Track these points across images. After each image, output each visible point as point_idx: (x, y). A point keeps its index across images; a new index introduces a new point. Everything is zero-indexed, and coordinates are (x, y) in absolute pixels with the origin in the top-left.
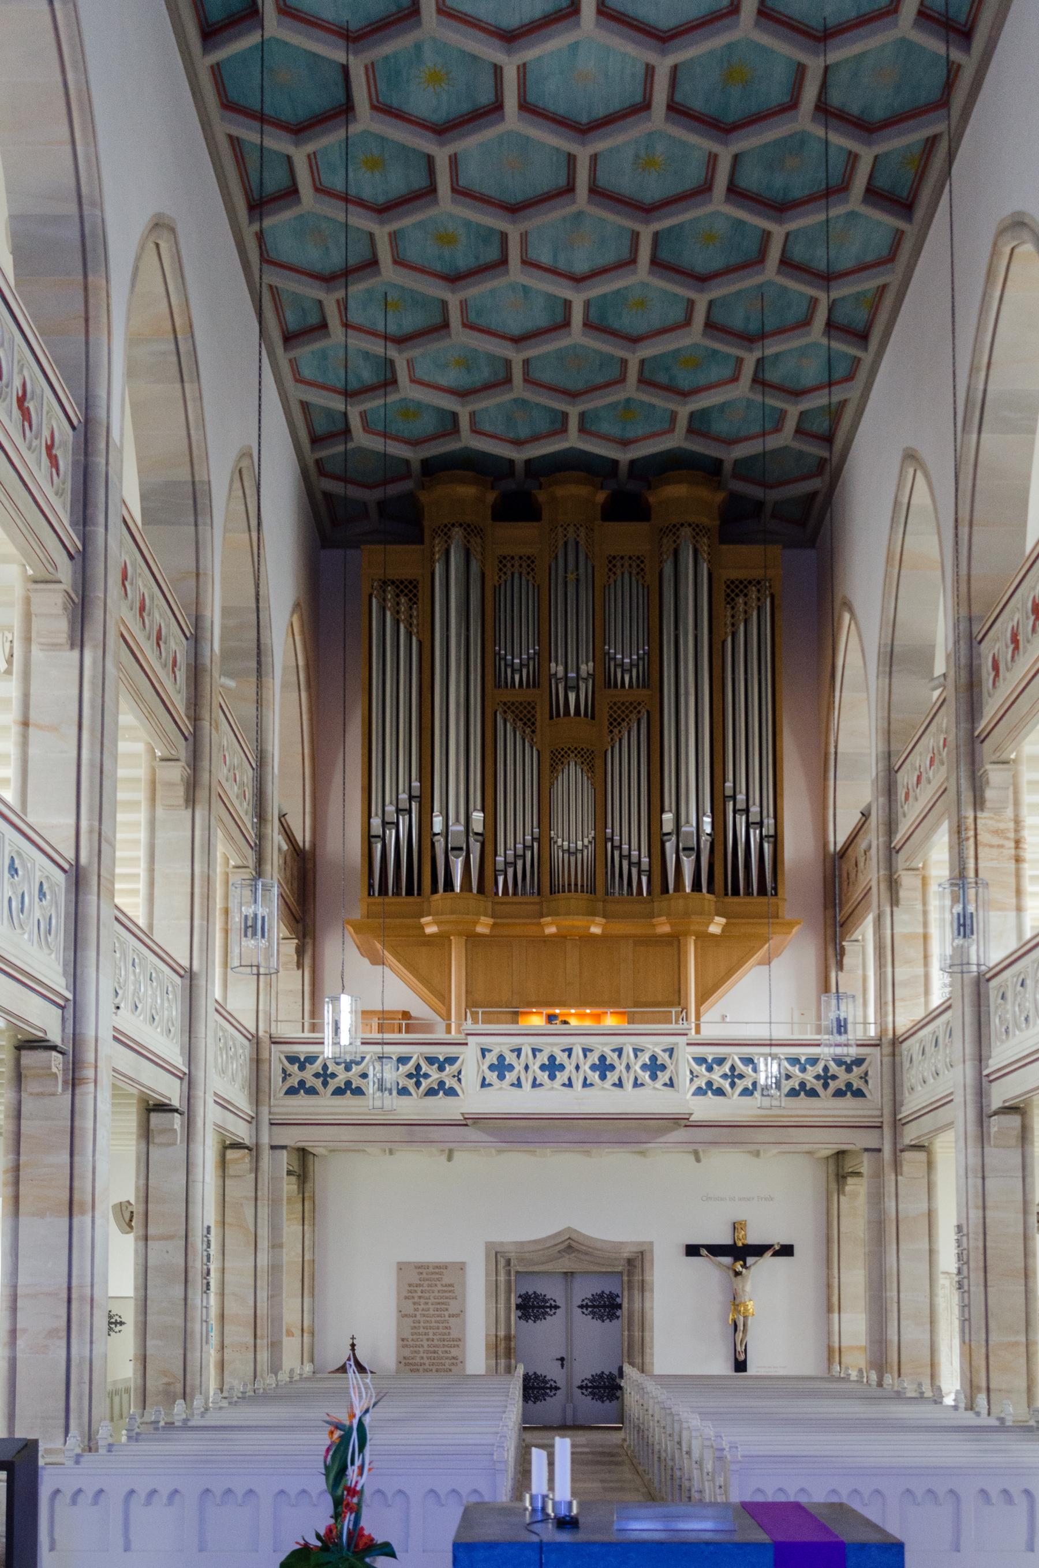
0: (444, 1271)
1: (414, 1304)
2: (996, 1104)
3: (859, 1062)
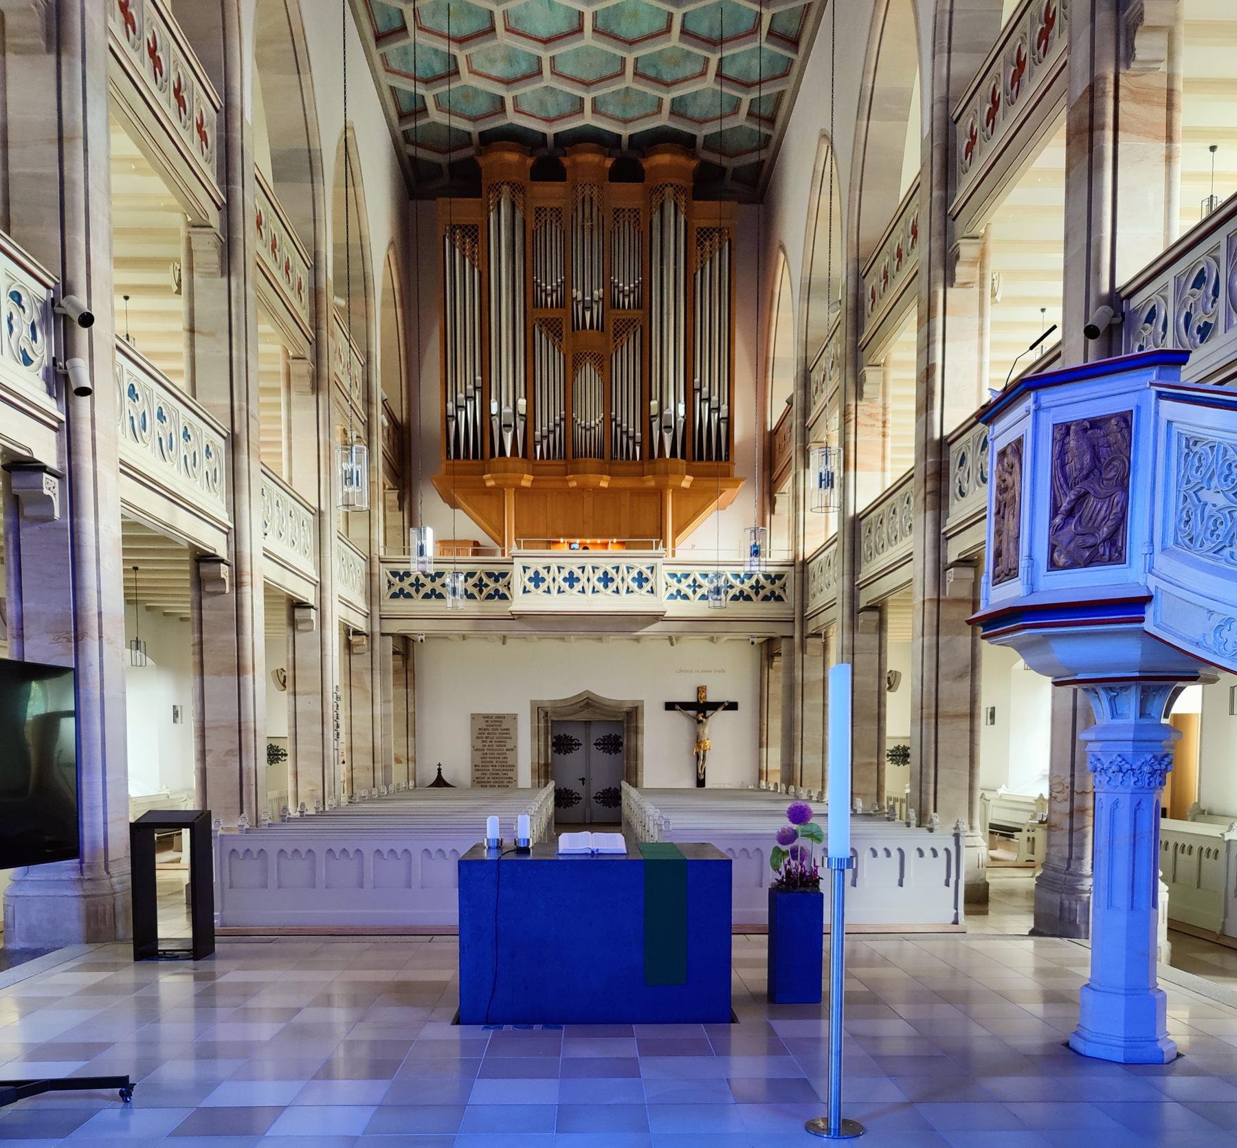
2: (862, 604)
3: (779, 576)
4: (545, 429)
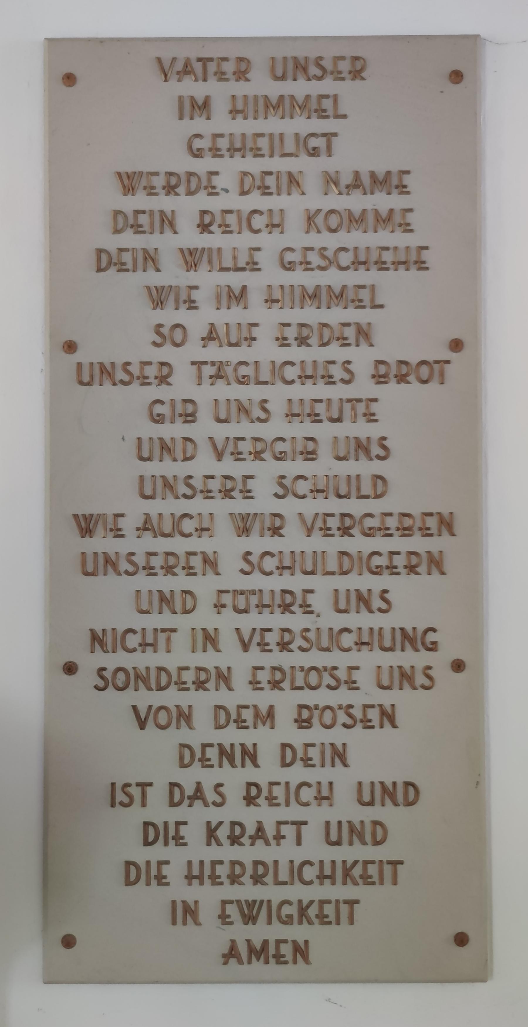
0: (346, 90)
1: (158, 297)
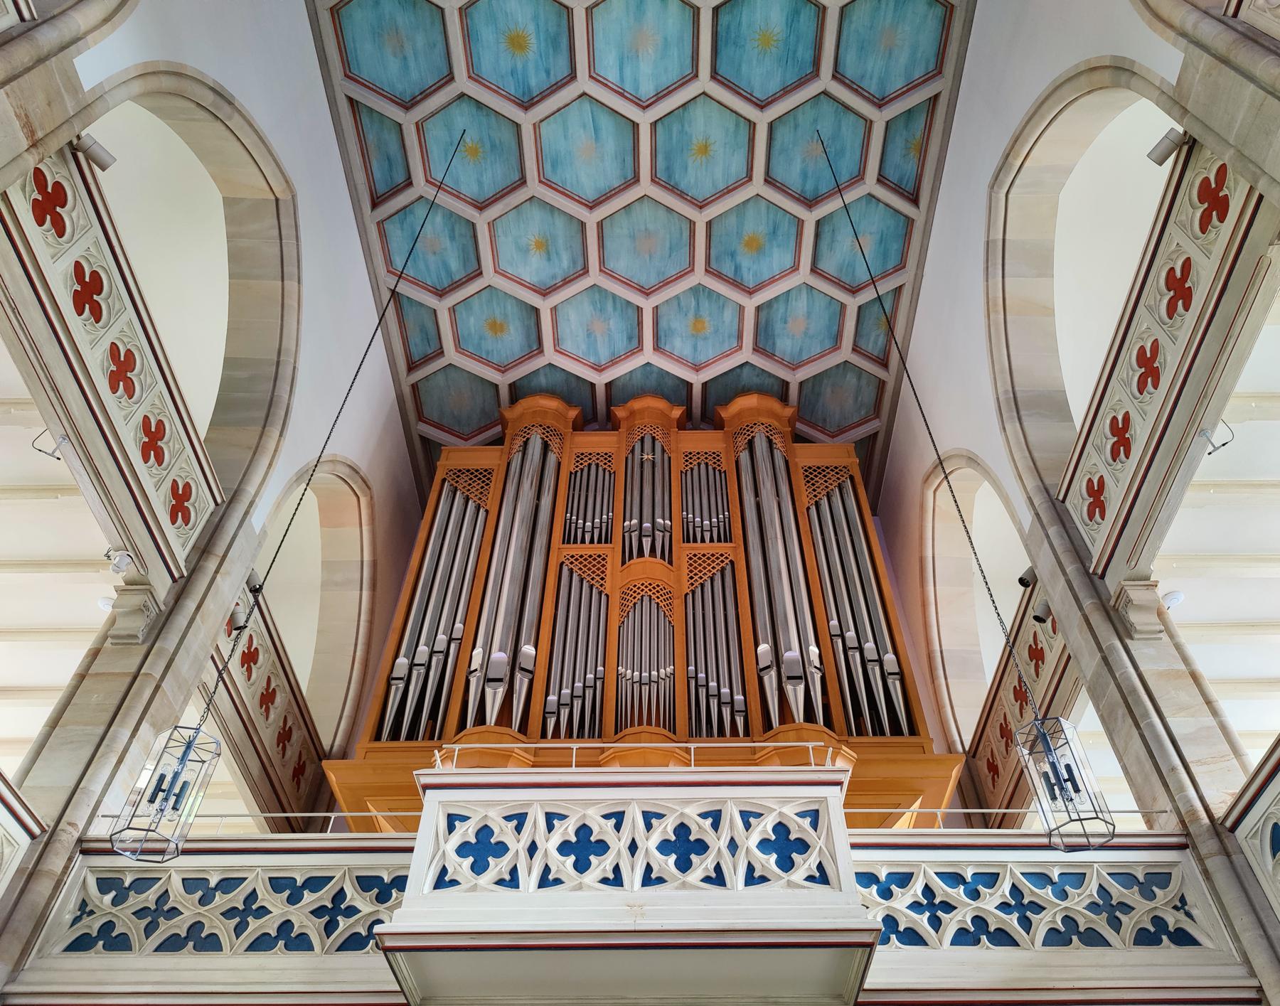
3: (1160, 878)
4: (566, 691)
